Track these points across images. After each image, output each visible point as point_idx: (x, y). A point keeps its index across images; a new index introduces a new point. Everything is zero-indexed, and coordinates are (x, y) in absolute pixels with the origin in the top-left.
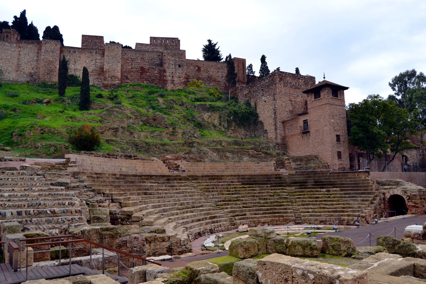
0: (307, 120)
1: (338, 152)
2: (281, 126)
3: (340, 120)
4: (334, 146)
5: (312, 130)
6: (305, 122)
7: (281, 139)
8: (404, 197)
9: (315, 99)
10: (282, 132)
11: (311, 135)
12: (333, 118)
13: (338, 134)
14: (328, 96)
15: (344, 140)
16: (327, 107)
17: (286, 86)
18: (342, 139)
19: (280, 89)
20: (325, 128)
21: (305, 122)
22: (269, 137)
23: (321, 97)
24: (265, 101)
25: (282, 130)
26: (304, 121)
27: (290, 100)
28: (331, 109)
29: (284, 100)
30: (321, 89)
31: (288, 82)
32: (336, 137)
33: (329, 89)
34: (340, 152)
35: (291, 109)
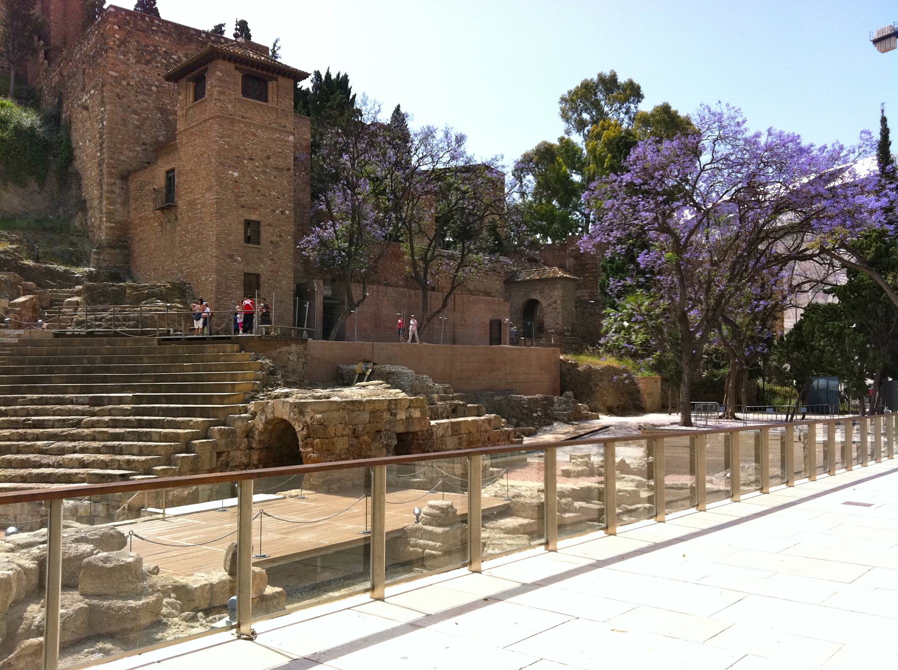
0: (173, 170)
1: (246, 275)
3: (265, 172)
4: (231, 256)
5: (181, 203)
6: (170, 176)
7: (111, 228)
8: (298, 428)
12: (237, 163)
13: (253, 217)
14: (222, 93)
16: (216, 127)
17: (148, 62)
18: (266, 235)
19: (122, 67)
20: (208, 195)
21: (170, 176)
22: (89, 223)
23: (206, 96)
24: (86, 108)
25: (119, 200)
26: (168, 172)
27: (162, 110)
28: (229, 136)
29: (135, 106)
30: (206, 70)
32: (241, 228)
33: (232, 66)
34: (258, 276)
35: (161, 138)
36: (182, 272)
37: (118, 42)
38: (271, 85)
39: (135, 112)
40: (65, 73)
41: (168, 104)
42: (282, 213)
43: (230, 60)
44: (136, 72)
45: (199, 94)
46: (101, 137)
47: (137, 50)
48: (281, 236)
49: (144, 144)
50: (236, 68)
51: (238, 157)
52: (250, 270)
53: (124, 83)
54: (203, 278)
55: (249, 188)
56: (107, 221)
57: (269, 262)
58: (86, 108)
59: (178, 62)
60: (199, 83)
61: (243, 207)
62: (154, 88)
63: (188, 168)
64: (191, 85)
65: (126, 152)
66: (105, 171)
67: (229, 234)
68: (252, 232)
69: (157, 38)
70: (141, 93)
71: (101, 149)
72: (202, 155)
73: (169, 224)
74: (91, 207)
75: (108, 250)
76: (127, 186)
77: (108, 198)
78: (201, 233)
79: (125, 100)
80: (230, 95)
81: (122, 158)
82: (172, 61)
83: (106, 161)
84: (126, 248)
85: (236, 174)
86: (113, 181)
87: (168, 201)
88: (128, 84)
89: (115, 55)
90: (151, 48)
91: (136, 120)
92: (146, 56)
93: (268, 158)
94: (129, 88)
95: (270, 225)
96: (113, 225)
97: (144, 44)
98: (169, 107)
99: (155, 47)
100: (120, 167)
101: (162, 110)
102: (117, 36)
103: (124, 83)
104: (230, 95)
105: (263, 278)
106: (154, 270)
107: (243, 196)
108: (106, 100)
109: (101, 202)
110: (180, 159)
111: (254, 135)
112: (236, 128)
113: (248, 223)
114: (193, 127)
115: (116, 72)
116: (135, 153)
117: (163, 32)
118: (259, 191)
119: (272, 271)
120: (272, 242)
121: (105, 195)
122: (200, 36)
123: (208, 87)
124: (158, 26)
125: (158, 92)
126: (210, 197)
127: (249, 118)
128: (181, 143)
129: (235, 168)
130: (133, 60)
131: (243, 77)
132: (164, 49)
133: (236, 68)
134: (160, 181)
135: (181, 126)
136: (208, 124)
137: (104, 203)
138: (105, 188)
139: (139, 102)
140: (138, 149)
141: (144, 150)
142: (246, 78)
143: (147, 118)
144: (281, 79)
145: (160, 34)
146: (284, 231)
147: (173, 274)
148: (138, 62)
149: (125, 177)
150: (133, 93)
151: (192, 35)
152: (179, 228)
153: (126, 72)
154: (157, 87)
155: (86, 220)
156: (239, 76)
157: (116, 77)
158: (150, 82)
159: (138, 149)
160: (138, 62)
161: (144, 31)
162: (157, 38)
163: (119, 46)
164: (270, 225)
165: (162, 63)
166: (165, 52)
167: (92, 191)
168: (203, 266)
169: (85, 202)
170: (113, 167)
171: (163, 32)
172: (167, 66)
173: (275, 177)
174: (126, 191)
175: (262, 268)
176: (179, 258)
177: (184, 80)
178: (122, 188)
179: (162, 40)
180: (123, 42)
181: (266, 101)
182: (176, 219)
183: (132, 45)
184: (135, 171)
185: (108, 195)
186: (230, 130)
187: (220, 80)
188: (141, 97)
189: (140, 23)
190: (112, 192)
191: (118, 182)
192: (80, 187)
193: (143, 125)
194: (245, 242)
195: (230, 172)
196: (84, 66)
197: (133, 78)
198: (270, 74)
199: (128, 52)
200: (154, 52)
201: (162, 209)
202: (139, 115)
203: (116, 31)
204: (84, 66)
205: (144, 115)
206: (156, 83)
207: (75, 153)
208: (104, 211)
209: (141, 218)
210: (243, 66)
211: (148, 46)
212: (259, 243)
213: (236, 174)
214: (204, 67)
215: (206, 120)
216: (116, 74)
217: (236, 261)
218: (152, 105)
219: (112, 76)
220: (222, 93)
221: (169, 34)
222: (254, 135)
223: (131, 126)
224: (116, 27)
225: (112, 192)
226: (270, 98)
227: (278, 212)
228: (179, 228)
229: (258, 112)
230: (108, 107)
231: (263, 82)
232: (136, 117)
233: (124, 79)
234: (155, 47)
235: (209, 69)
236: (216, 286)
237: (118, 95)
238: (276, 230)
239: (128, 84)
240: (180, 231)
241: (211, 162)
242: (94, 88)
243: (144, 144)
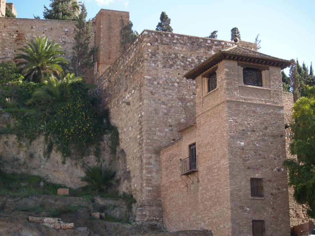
0: (194, 144)
1: (254, 221)
2: (152, 161)
3: (263, 140)
4: (242, 208)
5: (201, 167)
6: (192, 148)
7: (150, 191)
9: (209, 91)
10: (154, 174)
11: (200, 179)
13: (257, 176)
15: (274, 191)
17: (171, 66)
18: (268, 189)
21: (192, 148)
22: (133, 188)
23: (218, 87)
24: (128, 104)
26: (190, 146)
27: (182, 99)
29: (164, 99)
30: (217, 68)
31: (176, 57)
32: (249, 184)
33: (235, 63)
34: (262, 222)
35: (182, 121)
36: (205, 221)
37: (150, 55)
38: (264, 73)
39: (163, 103)
40: (112, 79)
41: (187, 94)
42: (279, 170)
43: (233, 59)
44: (163, 74)
45: (212, 86)
46: (140, 124)
47: (163, 58)
48: (279, 189)
49: (170, 126)
50: (238, 65)
51: (244, 130)
52: (256, 218)
53: (155, 83)
54: (221, 226)
55: (252, 152)
56: (146, 186)
57: (270, 210)
58: (128, 104)
59: (192, 63)
60: (212, 77)
61: (249, 168)
62: (176, 84)
63: (206, 142)
64: (206, 80)
65: (158, 133)
66: (144, 148)
67: (239, 190)
68: (256, 187)
69: (176, 48)
70: (167, 89)
71: (141, 133)
72: (216, 131)
73: (192, 186)
74: (134, 176)
75: (148, 208)
76: (160, 158)
77: (147, 169)
78: (219, 191)
79: (156, 95)
80: (235, 84)
81: (155, 138)
82: (188, 63)
83: (145, 141)
84: (160, 205)
85: (242, 144)
86: (150, 155)
87: (191, 167)
88: (158, 83)
89: (149, 64)
90: (173, 56)
91: (165, 109)
92: (169, 62)
93: (266, 128)
94: (159, 86)
95: (270, 181)
96: (151, 188)
97: (167, 53)
98: (187, 97)
99: (176, 54)
100: (154, 145)
101: (182, 99)
102: (150, 50)
103: (155, 83)
104: (235, 84)
105: (267, 224)
106: (183, 222)
107: (248, 160)
108: (143, 97)
109: (141, 172)
110: (199, 136)
111: (254, 112)
112: (241, 109)
113: (254, 181)
114: (209, 111)
115: (150, 76)
116: (164, 133)
117: (181, 43)
118: (260, 155)
119: (273, 217)
120: (272, 194)
121: (145, 166)
122: (206, 42)
123: (219, 79)
124: (177, 39)
125: (179, 86)
126: (225, 163)
127: (250, 100)
128: (200, 123)
129: (241, 139)
130: (160, 66)
131: (243, 70)
132: (182, 55)
133: (238, 65)
134: (185, 154)
135: (199, 111)
136: (220, 108)
137: (144, 172)
138: (144, 161)
139: (166, 95)
140: (167, 130)
141: (171, 130)
142: (246, 70)
143: (172, 107)
144: (271, 68)
145: (179, 45)
146: (281, 185)
147: (197, 224)
148: (164, 67)
149: (158, 152)
150: (162, 89)
151: (201, 42)
152: (200, 188)
153: (157, 75)
154: (178, 83)
155: (130, 186)
156: (241, 69)
157: (150, 80)
158: (173, 80)
159: (167, 130)
160: (164, 67)
161: (167, 44)
162: (176, 48)
163: (151, 58)
164: (270, 181)
165: (181, 66)
166: (183, 57)
167: (133, 165)
168: (221, 216)
169: (129, 172)
170: (149, 145)
171: (181, 43)
172: (184, 67)
173: (272, 143)
174: (159, 162)
175: (265, 215)
176: (202, 211)
177: (199, 78)
178: (156, 161)
179: (180, 49)
180: (154, 54)
181: (261, 86)
182: (198, 181)
183: (160, 56)
184: (166, 147)
185: (147, 166)
186: (238, 110)
187: (227, 74)
188: (167, 92)
189: (165, 39)
190: (149, 164)
191: (154, 156)
192: (125, 161)
193: (169, 111)
194: (253, 195)
195: (238, 142)
196: (126, 74)
197: (162, 78)
198: (263, 65)
199: (157, 61)
200: (175, 58)
201: (187, 174)
202: (166, 105)
203: (149, 47)
204: (126, 74)
205: (170, 105)
206: (178, 80)
207: (120, 137)
208: (144, 178)
209: (171, 182)
210: (243, 63)
211: (171, 55)
212: (262, 196)
213: (242, 144)
214: (215, 66)
215: (218, 105)
216: (150, 77)
217: (246, 211)
218: (175, 97)
219: (147, 79)
220: (228, 84)
221: (185, 44)
222: (254, 112)
223: (161, 114)
224: (149, 44)
225: (149, 164)
226: (264, 83)
227: (275, 170)
228: (200, 188)
229: (257, 95)
230: (145, 101)
231: (258, 71)
232: (164, 106)
233: (155, 80)
234: (176, 54)
235: (219, 67)
236: (232, 232)
237: (152, 93)
238: (275, 184)
239: (158, 83)
240: (201, 191)
241: (223, 136)
242: (134, 88)
243: (170, 126)
